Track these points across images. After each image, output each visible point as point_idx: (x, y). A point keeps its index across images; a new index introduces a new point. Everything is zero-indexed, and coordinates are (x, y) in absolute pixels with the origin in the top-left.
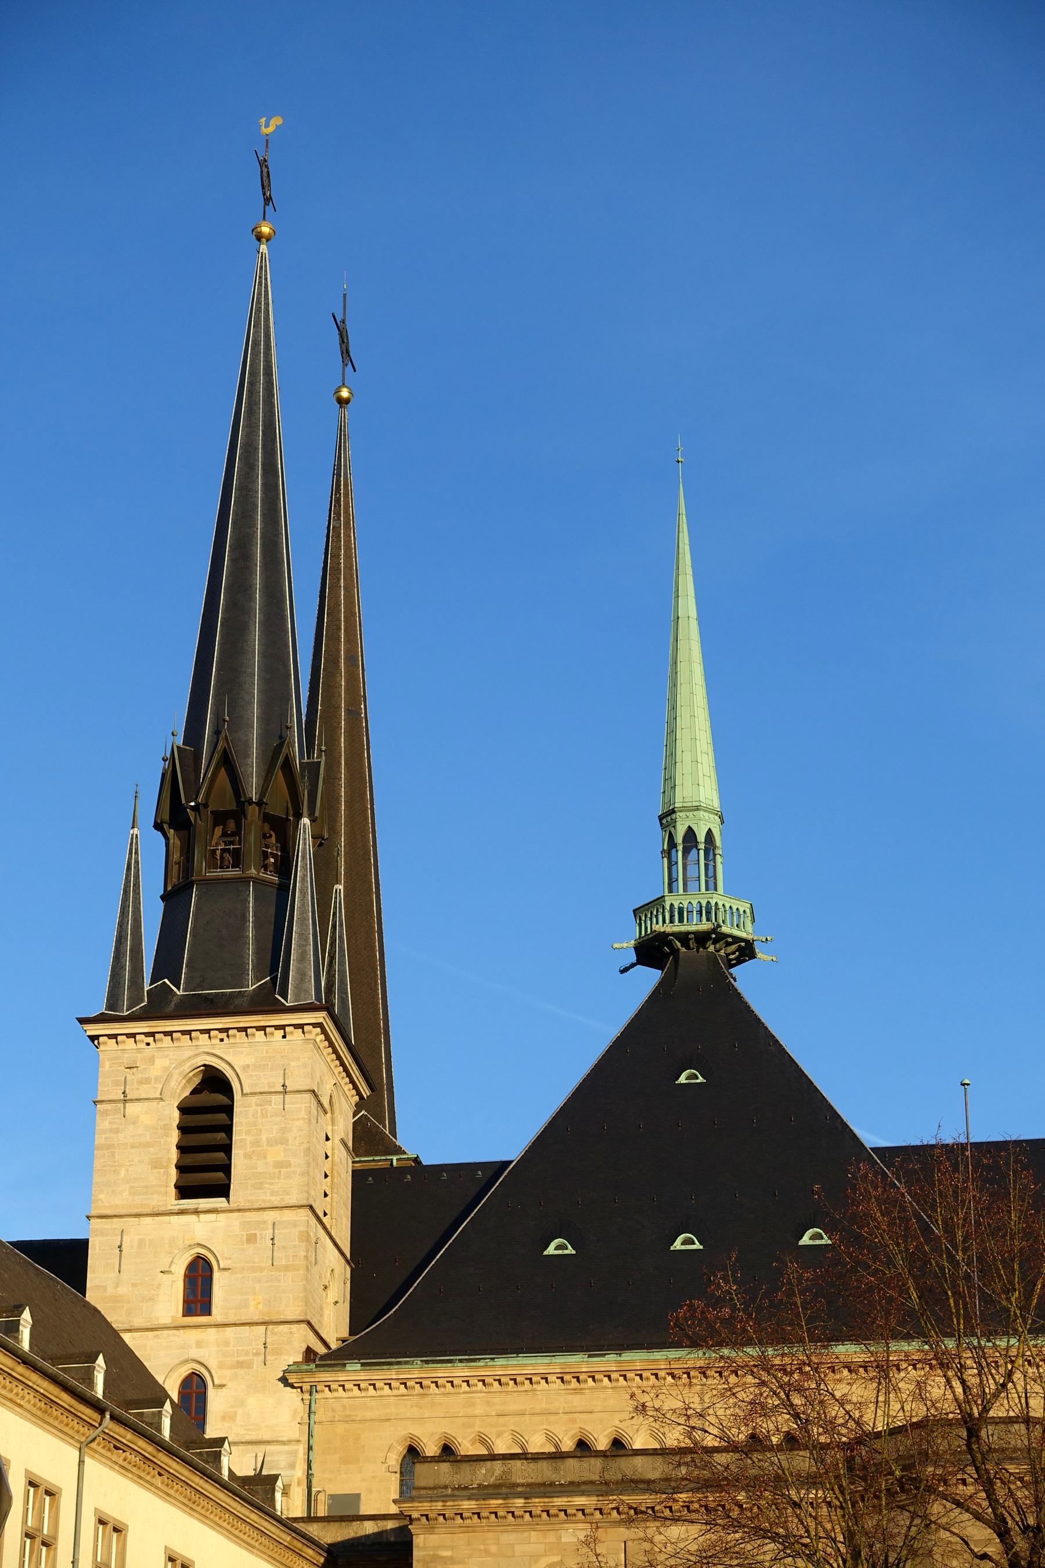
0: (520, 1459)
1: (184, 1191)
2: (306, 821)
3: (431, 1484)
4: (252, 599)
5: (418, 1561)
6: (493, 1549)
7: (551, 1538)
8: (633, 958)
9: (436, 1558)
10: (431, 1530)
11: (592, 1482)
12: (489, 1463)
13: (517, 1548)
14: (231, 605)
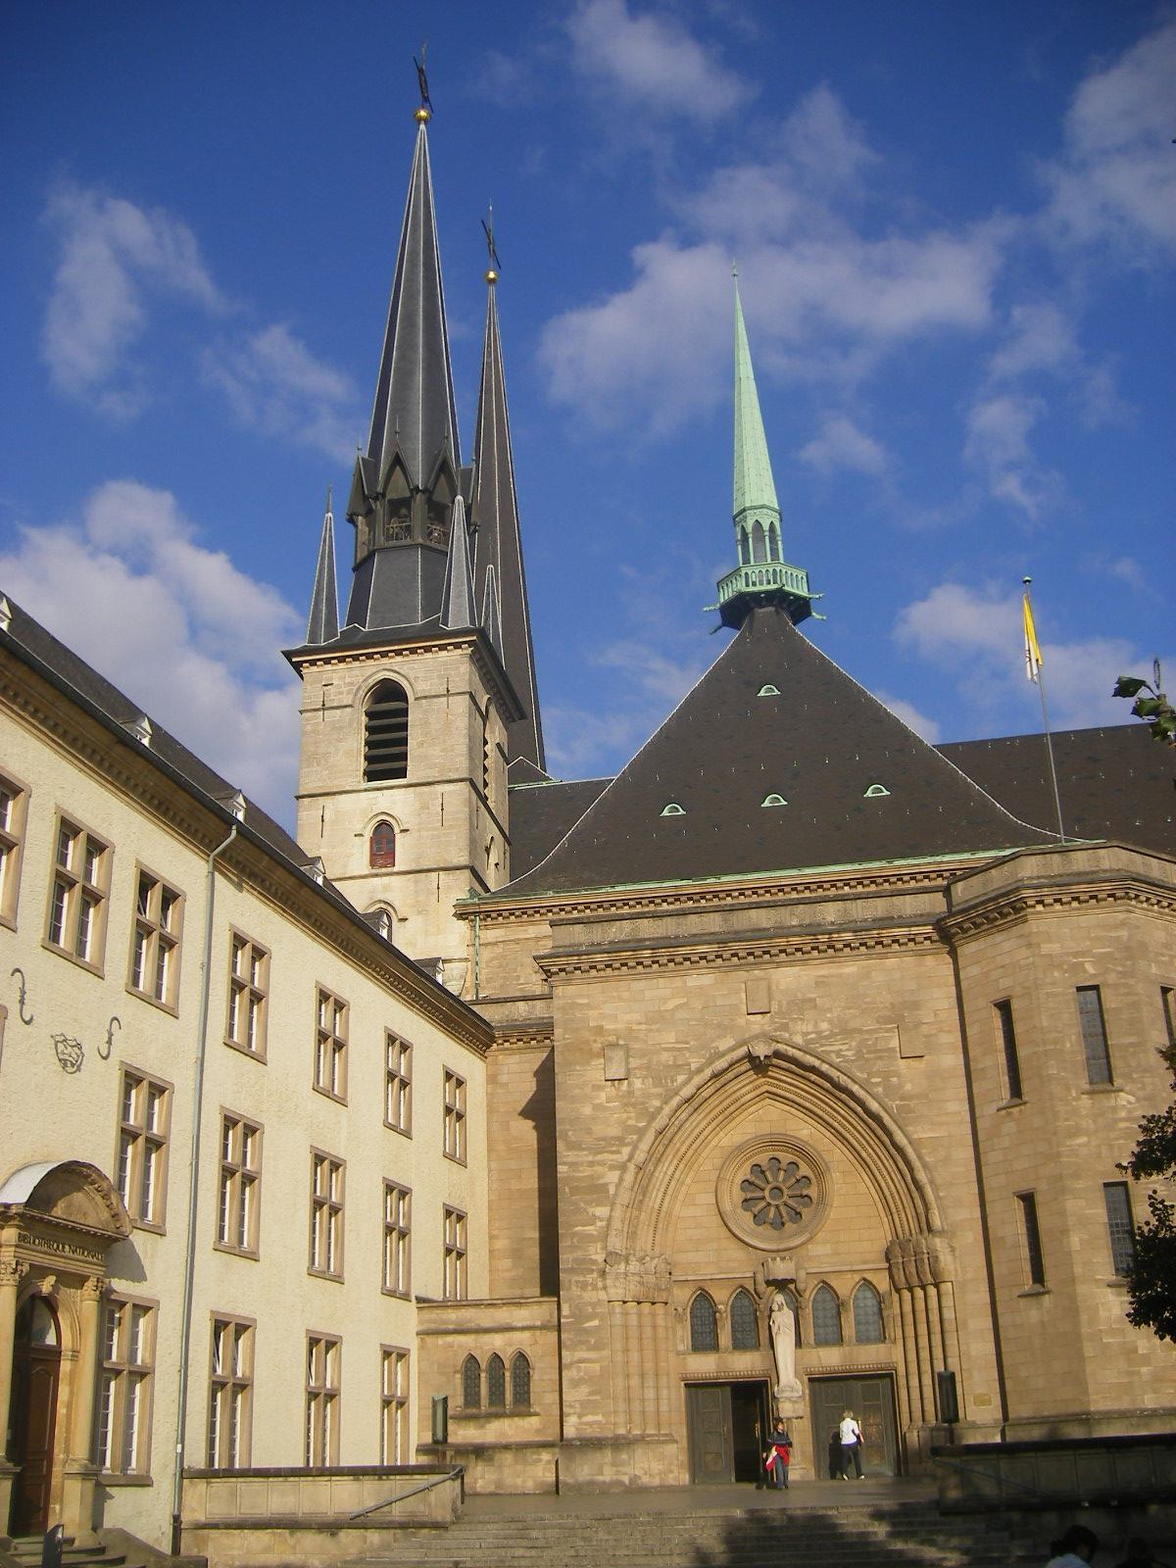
1: (371, 775)
2: (459, 498)
4: (416, 351)
5: (558, 1009)
7: (678, 982)
8: (719, 621)
9: (574, 1005)
10: (568, 982)
13: (646, 992)
14: (401, 358)
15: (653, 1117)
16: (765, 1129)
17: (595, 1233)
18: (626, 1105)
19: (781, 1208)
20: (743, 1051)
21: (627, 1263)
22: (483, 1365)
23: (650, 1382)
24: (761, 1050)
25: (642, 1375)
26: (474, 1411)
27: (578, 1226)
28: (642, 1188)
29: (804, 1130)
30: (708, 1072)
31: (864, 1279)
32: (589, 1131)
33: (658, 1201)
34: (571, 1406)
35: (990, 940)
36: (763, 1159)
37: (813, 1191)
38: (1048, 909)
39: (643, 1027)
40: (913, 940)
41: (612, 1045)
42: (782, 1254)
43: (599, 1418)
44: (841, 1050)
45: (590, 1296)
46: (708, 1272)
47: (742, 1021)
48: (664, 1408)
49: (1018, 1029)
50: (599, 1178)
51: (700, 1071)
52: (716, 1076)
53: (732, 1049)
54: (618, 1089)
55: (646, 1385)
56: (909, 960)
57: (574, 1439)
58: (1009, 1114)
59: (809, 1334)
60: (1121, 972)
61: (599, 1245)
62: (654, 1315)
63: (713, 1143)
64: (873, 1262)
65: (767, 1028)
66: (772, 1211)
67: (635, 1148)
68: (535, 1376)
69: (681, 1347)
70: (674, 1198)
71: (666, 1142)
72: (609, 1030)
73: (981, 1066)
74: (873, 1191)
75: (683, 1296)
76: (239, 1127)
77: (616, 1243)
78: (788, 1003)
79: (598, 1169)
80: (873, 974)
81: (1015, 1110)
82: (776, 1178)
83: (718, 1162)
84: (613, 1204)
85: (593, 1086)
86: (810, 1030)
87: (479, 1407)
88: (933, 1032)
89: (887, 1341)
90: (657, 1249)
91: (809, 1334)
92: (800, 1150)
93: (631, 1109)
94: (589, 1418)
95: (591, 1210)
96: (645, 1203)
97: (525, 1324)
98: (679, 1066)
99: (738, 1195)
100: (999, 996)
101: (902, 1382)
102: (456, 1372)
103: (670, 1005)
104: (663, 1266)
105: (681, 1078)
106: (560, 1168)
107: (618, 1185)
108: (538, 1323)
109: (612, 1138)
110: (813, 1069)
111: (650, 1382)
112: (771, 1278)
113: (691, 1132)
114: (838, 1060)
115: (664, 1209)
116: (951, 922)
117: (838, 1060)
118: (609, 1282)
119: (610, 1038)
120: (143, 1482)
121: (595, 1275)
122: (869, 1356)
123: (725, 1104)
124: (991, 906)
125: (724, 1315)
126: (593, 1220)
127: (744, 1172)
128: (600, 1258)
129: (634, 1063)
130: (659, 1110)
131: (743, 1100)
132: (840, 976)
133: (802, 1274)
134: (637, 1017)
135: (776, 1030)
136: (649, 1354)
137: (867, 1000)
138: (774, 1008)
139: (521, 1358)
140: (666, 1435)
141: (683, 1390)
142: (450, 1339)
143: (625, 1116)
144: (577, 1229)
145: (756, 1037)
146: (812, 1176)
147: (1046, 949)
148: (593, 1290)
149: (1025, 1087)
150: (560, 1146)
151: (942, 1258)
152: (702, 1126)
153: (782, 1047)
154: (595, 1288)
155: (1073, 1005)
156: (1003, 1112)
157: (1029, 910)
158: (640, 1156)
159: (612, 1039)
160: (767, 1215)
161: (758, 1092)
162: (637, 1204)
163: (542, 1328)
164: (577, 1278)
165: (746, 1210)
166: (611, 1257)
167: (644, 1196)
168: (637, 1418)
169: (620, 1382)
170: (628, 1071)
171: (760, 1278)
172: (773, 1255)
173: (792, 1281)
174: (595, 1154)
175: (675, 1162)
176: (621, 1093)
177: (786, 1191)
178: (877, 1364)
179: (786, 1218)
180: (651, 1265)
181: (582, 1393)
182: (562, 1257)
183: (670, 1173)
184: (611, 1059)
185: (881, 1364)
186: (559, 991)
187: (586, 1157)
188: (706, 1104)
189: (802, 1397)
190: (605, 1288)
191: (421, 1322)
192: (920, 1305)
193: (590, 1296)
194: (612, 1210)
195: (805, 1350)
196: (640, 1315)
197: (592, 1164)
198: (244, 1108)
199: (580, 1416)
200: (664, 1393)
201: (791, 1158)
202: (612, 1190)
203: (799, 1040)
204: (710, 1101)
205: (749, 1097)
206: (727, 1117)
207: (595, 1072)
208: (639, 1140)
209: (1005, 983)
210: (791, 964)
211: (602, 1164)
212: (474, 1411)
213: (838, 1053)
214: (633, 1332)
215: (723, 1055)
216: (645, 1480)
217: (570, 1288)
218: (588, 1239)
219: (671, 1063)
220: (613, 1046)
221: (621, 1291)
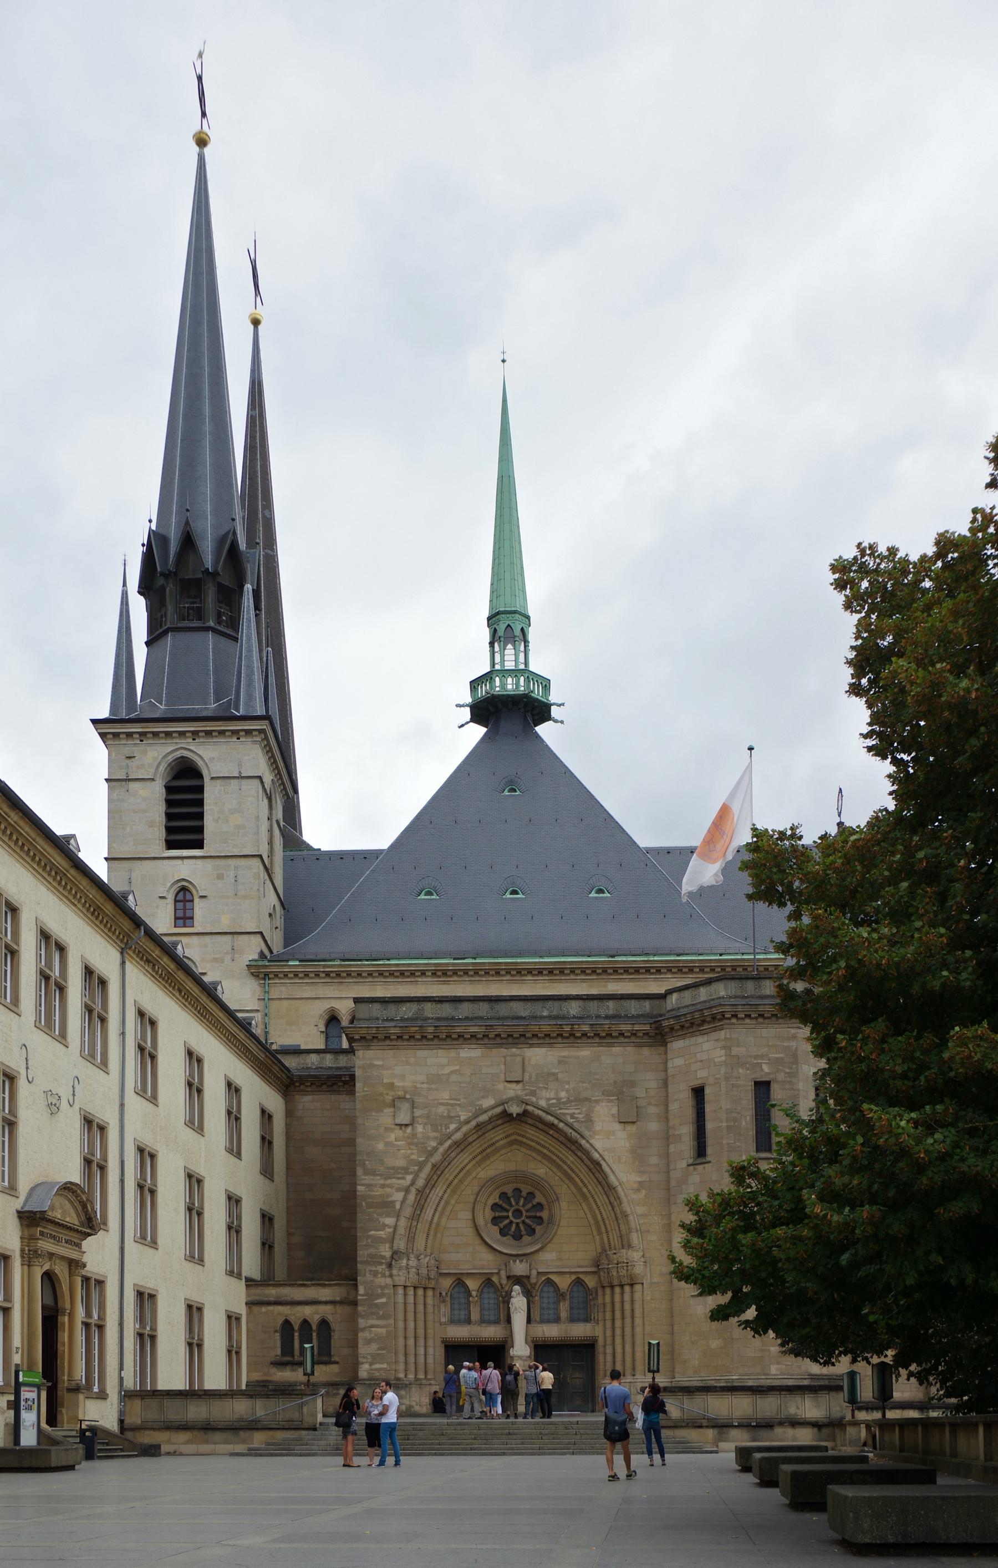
0: (430, 1001)
3: (367, 1016)
5: (359, 1067)
6: (412, 1060)
7: (453, 1053)
10: (368, 1048)
11: (481, 1018)
12: (408, 1004)
13: (428, 1060)
15: (431, 1154)
16: (512, 1167)
17: (384, 1236)
18: (410, 1144)
19: (521, 1225)
20: (499, 1110)
21: (408, 1259)
22: (296, 1327)
23: (421, 1342)
24: (515, 1109)
25: (416, 1338)
26: (289, 1359)
27: (371, 1230)
28: (420, 1206)
29: (541, 1170)
30: (473, 1123)
31: (578, 1278)
32: (381, 1162)
33: (431, 1215)
34: (364, 1357)
35: (693, 1040)
36: (509, 1189)
37: (544, 1214)
38: (740, 1022)
39: (425, 1086)
40: (635, 1034)
41: (399, 1098)
42: (521, 1258)
43: (385, 1366)
44: (574, 1113)
45: (380, 1281)
46: (466, 1268)
47: (501, 1086)
48: (430, 1360)
49: (708, 1108)
50: (390, 1195)
51: (467, 1122)
52: (479, 1126)
53: (493, 1108)
54: (405, 1132)
55: (418, 1344)
56: (630, 1049)
57: (364, 1380)
58: (694, 1169)
59: (536, 1315)
60: (787, 1073)
61: (387, 1246)
62: (425, 1296)
63: (474, 1174)
64: (586, 1267)
65: (519, 1093)
66: (514, 1226)
67: (416, 1175)
68: (335, 1336)
69: (443, 1320)
70: (442, 1214)
71: (439, 1173)
72: (398, 1087)
73: (677, 1133)
74: (589, 1216)
75: (447, 1283)
76: (146, 1156)
77: (401, 1244)
78: (537, 1075)
79: (388, 1190)
80: (603, 1058)
81: (700, 1168)
82: (517, 1203)
83: (476, 1189)
84: (398, 1217)
85: (385, 1128)
86: (552, 1097)
87: (293, 1356)
88: (645, 1104)
90: (429, 1251)
91: (536, 1315)
92: (537, 1183)
93: (414, 1147)
94: (377, 1366)
95: (382, 1220)
96: (422, 1215)
97: (328, 1299)
98: (452, 1117)
99: (489, 1214)
100: (696, 1083)
101: (600, 1349)
102: (276, 1331)
103: (447, 1070)
104: (433, 1262)
105: (452, 1127)
106: (359, 1188)
107: (403, 1202)
108: (338, 1299)
109: (399, 1168)
110: (552, 1126)
111: (421, 1342)
113: (457, 1167)
114: (572, 1121)
115: (435, 1221)
116: (665, 1023)
117: (572, 1121)
118: (395, 1272)
119: (399, 1093)
120: (102, 1396)
121: (384, 1266)
122: (579, 1331)
123: (484, 1147)
124: (697, 1015)
126: (384, 1226)
127: (494, 1198)
128: (388, 1254)
129: (418, 1113)
130: (435, 1149)
131: (497, 1145)
132: (578, 1057)
134: (422, 1078)
135: (526, 1095)
136: (421, 1324)
137: (597, 1077)
138: (527, 1078)
139: (324, 1323)
140: (430, 1379)
141: (443, 1350)
142: (271, 1308)
143: (409, 1152)
144: (372, 1233)
145: (511, 1099)
146: (544, 1202)
147: (735, 1051)
148: (382, 1277)
149: (709, 1150)
150: (359, 1171)
151: (637, 1267)
152: (466, 1162)
153: (530, 1108)
154: (384, 1276)
155: (750, 1094)
156: (691, 1168)
157: (726, 1021)
158: (420, 1182)
159: (400, 1093)
160: (510, 1229)
161: (509, 1139)
162: (415, 1217)
163: (341, 1303)
164: (370, 1268)
165: (494, 1224)
166: (396, 1254)
167: (421, 1211)
168: (412, 1367)
169: (401, 1341)
170: (413, 1118)
171: (503, 1273)
172: (514, 1258)
173: (528, 1277)
174: (386, 1179)
175: (445, 1187)
176: (406, 1135)
177: (524, 1214)
179: (523, 1232)
180: (425, 1261)
181: (374, 1347)
182: (360, 1252)
183: (440, 1195)
184: (400, 1109)
186: (360, 1053)
187: (380, 1181)
188: (470, 1147)
189: (529, 1357)
190: (391, 1276)
191: (248, 1295)
192: (617, 1298)
193: (380, 1281)
194: (397, 1220)
196: (415, 1295)
197: (383, 1186)
198: (149, 1142)
199: (371, 1364)
200: (431, 1351)
201: (530, 1189)
202: (398, 1206)
203: (543, 1103)
204: (474, 1144)
205: (501, 1143)
206: (484, 1156)
207: (386, 1118)
208: (420, 1170)
209: (702, 1074)
210: (539, 1045)
211: (391, 1186)
212: (289, 1359)
213: (572, 1116)
214: (411, 1308)
215: (486, 1112)
216: (417, 1408)
217: (365, 1275)
218: (380, 1240)
219: (445, 1114)
220: (403, 1098)
221: (403, 1279)
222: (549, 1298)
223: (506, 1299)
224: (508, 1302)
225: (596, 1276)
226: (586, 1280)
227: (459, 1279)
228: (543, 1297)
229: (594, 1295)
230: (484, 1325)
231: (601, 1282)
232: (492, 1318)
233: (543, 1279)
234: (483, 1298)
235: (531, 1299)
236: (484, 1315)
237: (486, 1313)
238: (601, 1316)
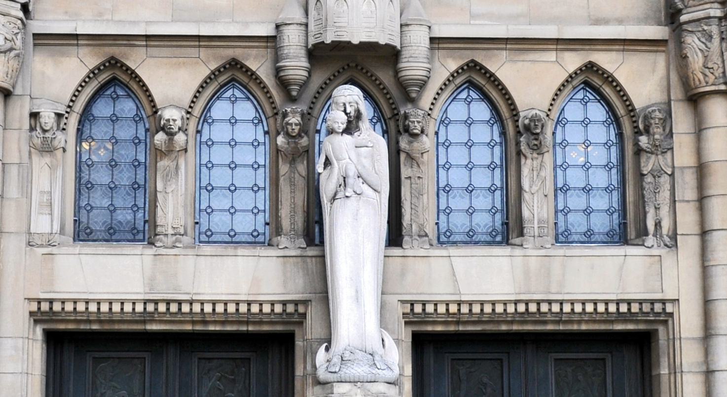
31: (591, 67)
64: (620, 21)
69: (42, 224)
89: (650, 240)
112: (329, 38)
125: (180, 138)
133: (418, 40)
178: (618, 302)
185: (629, 302)
195: (411, 247)
222: (469, 145)
223: (304, 141)
224: (308, 154)
225: (660, 60)
226: (621, 77)
227: (113, 63)
228: (447, 145)
229: (658, 132)
230: (207, 249)
231: (685, 81)
232: (245, 224)
233: (453, 65)
234: (210, 143)
235: (404, 143)
236: (209, 211)
237: (220, 201)
238: (687, 219)
